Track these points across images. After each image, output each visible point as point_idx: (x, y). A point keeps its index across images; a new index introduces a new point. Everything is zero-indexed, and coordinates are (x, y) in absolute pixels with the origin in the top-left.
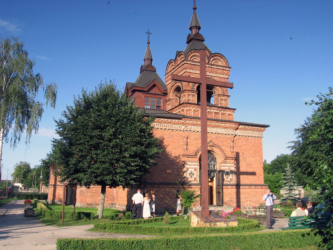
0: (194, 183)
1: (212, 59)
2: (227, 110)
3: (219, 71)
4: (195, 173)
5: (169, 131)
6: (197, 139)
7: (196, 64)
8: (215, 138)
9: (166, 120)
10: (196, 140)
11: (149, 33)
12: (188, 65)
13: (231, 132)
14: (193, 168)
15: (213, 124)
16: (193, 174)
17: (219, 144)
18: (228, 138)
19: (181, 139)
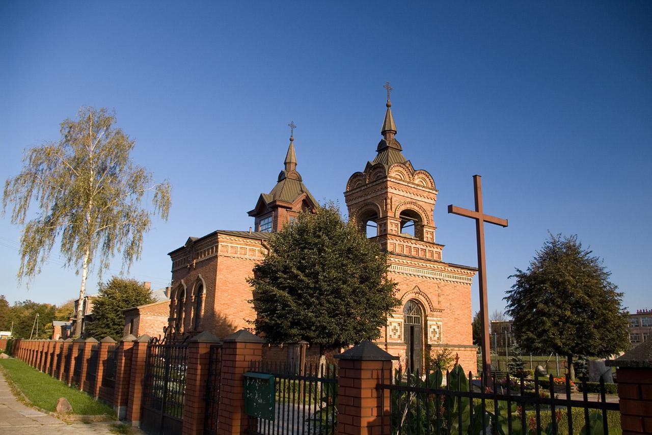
0: (398, 342)
6: (402, 283)
11: (292, 126)
12: (391, 183)
16: (397, 330)
17: (426, 291)
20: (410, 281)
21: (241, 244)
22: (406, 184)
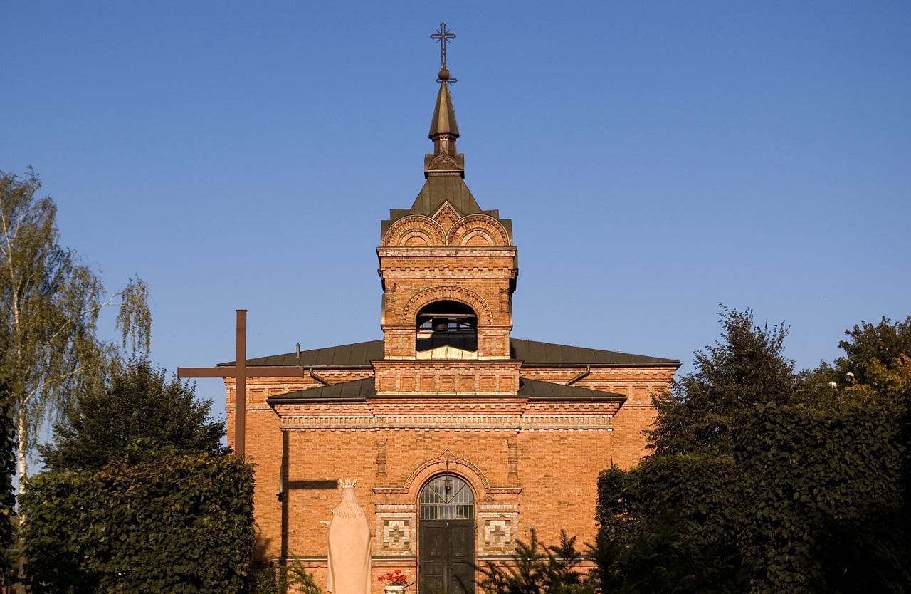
1: (461, 231)
2: (497, 366)
3: (481, 261)
4: (406, 530)
5: (338, 432)
6: (412, 447)
7: (410, 255)
8: (462, 441)
9: (326, 406)
10: (408, 449)
12: (389, 260)
13: (507, 421)
14: (400, 519)
15: (452, 406)
18: (499, 439)
19: (370, 449)
20: (433, 441)
21: (270, 383)
22: (428, 254)
